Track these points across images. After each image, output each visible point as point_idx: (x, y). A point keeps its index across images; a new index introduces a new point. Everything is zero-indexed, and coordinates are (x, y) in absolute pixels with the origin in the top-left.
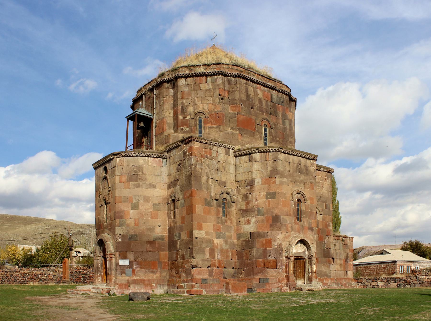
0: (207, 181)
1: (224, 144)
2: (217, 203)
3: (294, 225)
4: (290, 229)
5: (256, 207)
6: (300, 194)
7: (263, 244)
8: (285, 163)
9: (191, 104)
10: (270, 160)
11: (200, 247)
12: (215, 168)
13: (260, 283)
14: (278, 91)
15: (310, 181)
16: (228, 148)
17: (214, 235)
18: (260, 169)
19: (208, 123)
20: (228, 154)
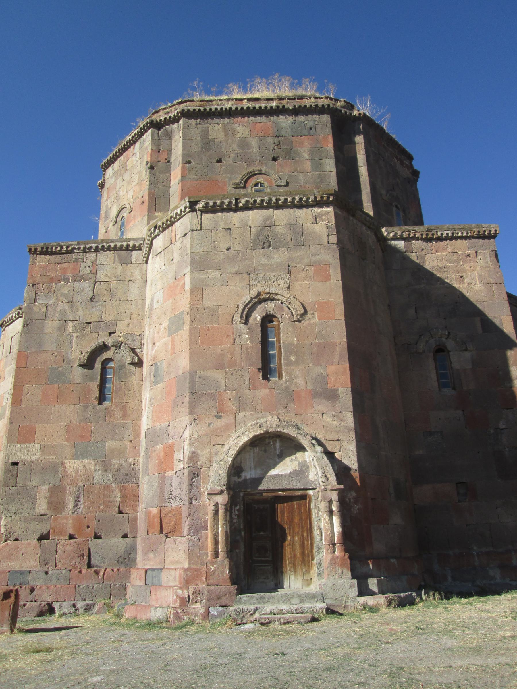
0: (62, 328)
1: (112, 245)
2: (84, 376)
3: (247, 391)
4: (230, 404)
5: (153, 362)
6: (273, 300)
7: (160, 463)
8: (213, 234)
9: (116, 201)
10: (177, 238)
11: (21, 485)
12: (84, 299)
13: (146, 584)
14: (296, 112)
15: (314, 259)
16: (127, 248)
17: (69, 451)
18: (162, 269)
19: (131, 220)
20: (126, 262)
